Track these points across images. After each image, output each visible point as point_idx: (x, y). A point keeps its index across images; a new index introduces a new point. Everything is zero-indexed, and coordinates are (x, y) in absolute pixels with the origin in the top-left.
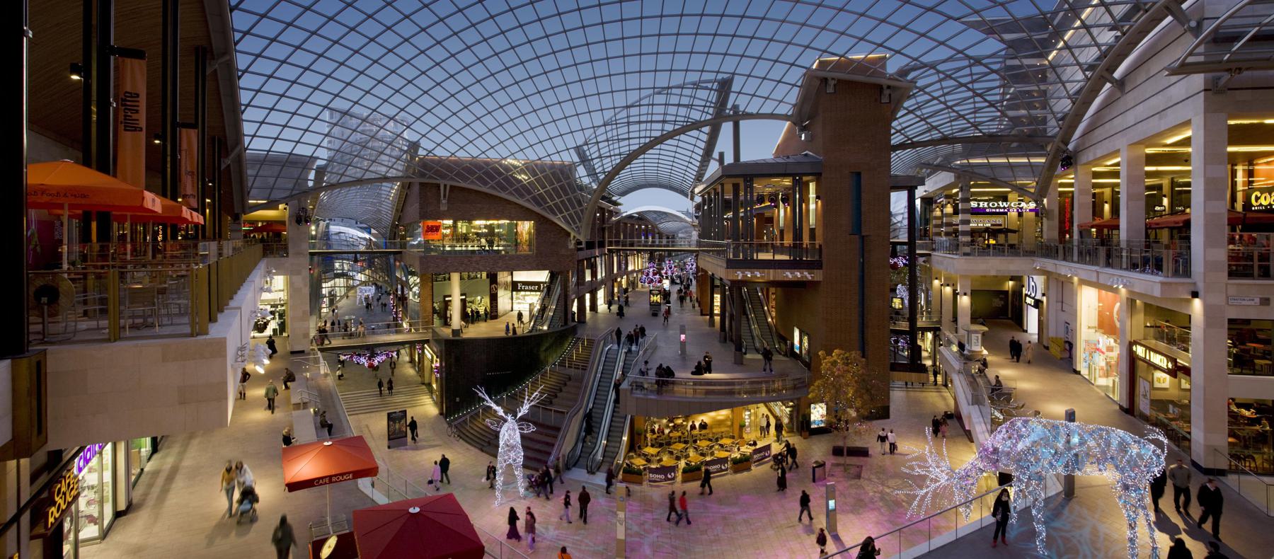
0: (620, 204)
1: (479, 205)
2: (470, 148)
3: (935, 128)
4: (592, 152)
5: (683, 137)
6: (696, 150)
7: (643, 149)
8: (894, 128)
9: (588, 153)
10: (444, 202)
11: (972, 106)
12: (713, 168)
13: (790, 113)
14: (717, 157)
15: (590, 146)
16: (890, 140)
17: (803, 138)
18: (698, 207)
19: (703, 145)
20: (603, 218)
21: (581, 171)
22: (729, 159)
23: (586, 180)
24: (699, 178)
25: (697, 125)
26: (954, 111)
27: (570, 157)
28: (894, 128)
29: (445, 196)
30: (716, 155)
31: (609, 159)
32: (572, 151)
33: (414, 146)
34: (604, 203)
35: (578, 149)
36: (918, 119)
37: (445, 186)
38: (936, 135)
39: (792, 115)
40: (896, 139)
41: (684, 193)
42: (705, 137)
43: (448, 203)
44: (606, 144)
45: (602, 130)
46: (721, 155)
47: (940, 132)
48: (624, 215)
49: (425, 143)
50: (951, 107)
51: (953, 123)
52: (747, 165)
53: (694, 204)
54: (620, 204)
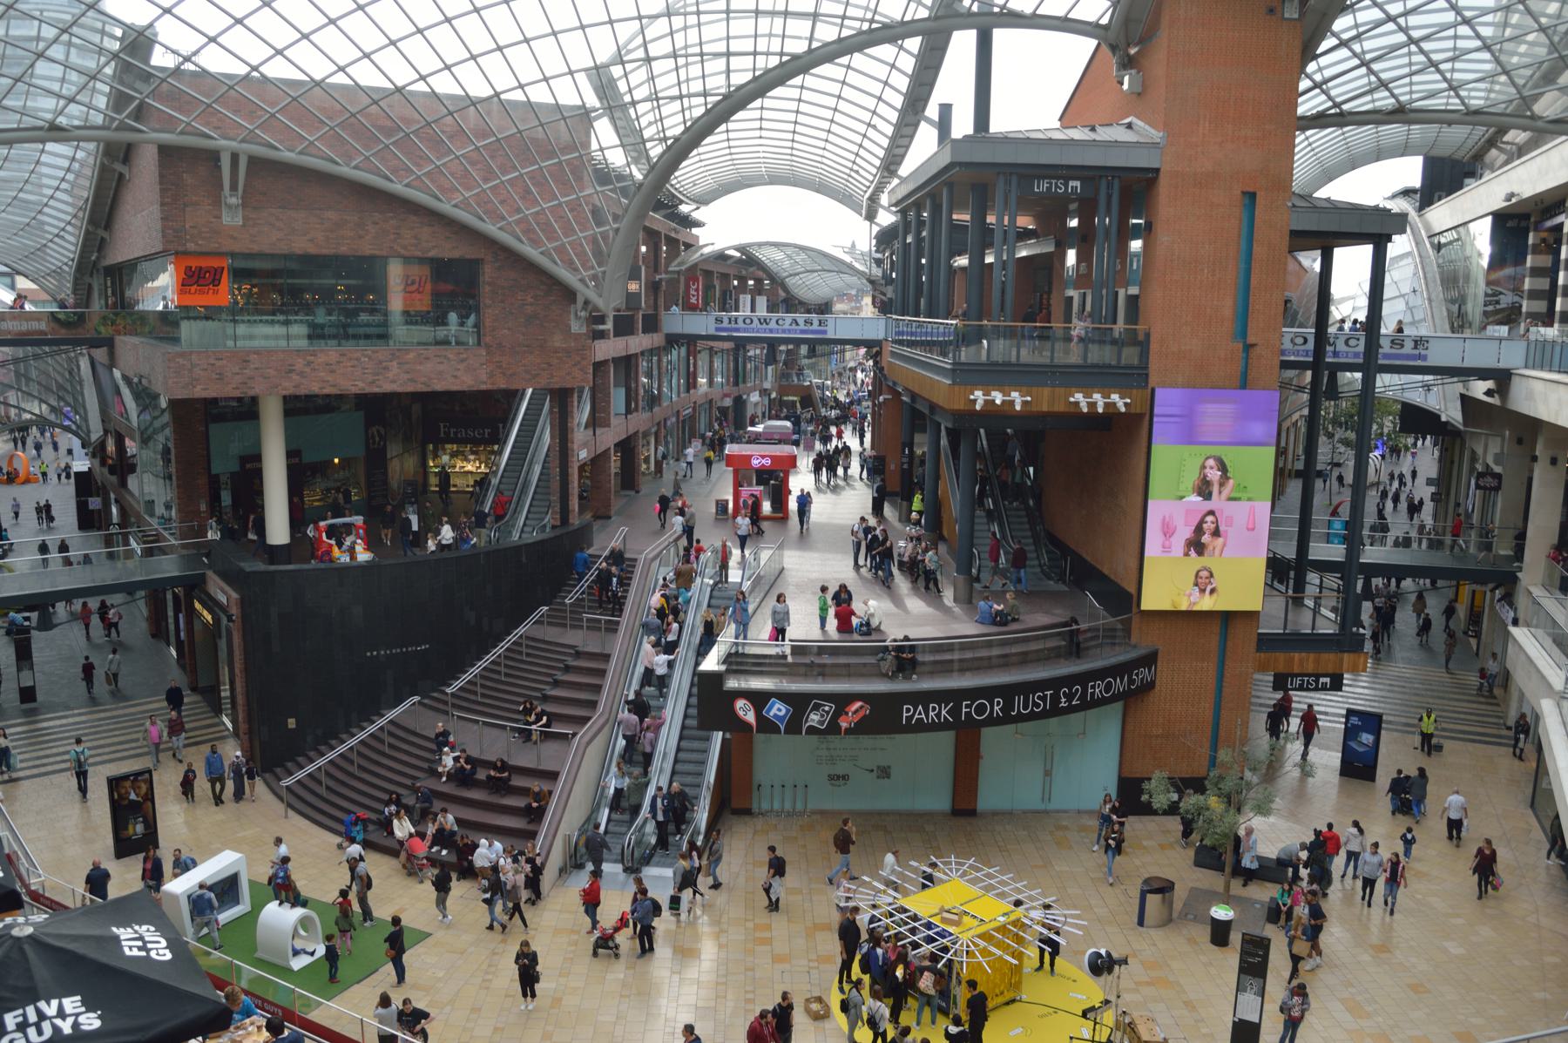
0: (698, 224)
1: (330, 214)
2: (302, 53)
3: (1384, 85)
4: (632, 82)
5: (858, 59)
6: (889, 95)
7: (762, 85)
8: (1308, 76)
9: (622, 86)
10: (233, 200)
11: (1450, 44)
12: (924, 147)
13: (1105, 21)
14: (936, 118)
15: (629, 67)
16: (1296, 105)
17: (1125, 86)
18: (885, 238)
19: (903, 83)
20: (654, 260)
21: (604, 133)
22: (963, 125)
23: (617, 158)
24: (890, 164)
25: (892, 33)
26: (1422, 51)
27: (574, 93)
28: (1308, 76)
29: (234, 187)
30: (932, 111)
31: (676, 105)
32: (582, 78)
33: (139, 42)
34: (657, 220)
35: (601, 78)
36: (1356, 62)
37: (235, 157)
38: (1383, 101)
39: (1106, 28)
40: (1308, 105)
41: (846, 199)
42: (908, 64)
43: (244, 205)
44: (670, 63)
45: (662, 26)
46: (946, 110)
47: (1393, 95)
48: (706, 250)
49: (168, 31)
50: (1416, 42)
51: (1415, 78)
52: (1005, 140)
53: (876, 229)
54: (698, 224)
